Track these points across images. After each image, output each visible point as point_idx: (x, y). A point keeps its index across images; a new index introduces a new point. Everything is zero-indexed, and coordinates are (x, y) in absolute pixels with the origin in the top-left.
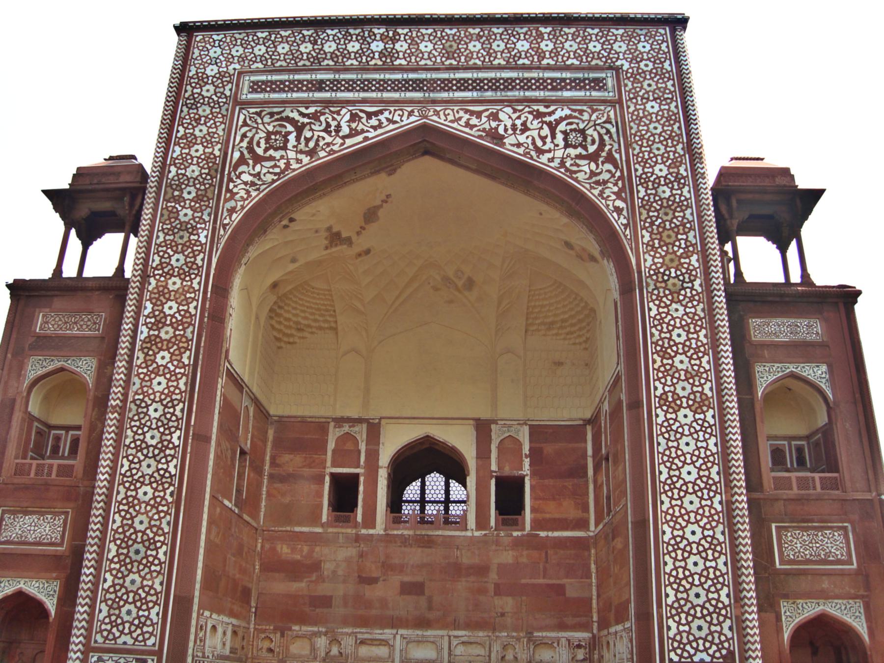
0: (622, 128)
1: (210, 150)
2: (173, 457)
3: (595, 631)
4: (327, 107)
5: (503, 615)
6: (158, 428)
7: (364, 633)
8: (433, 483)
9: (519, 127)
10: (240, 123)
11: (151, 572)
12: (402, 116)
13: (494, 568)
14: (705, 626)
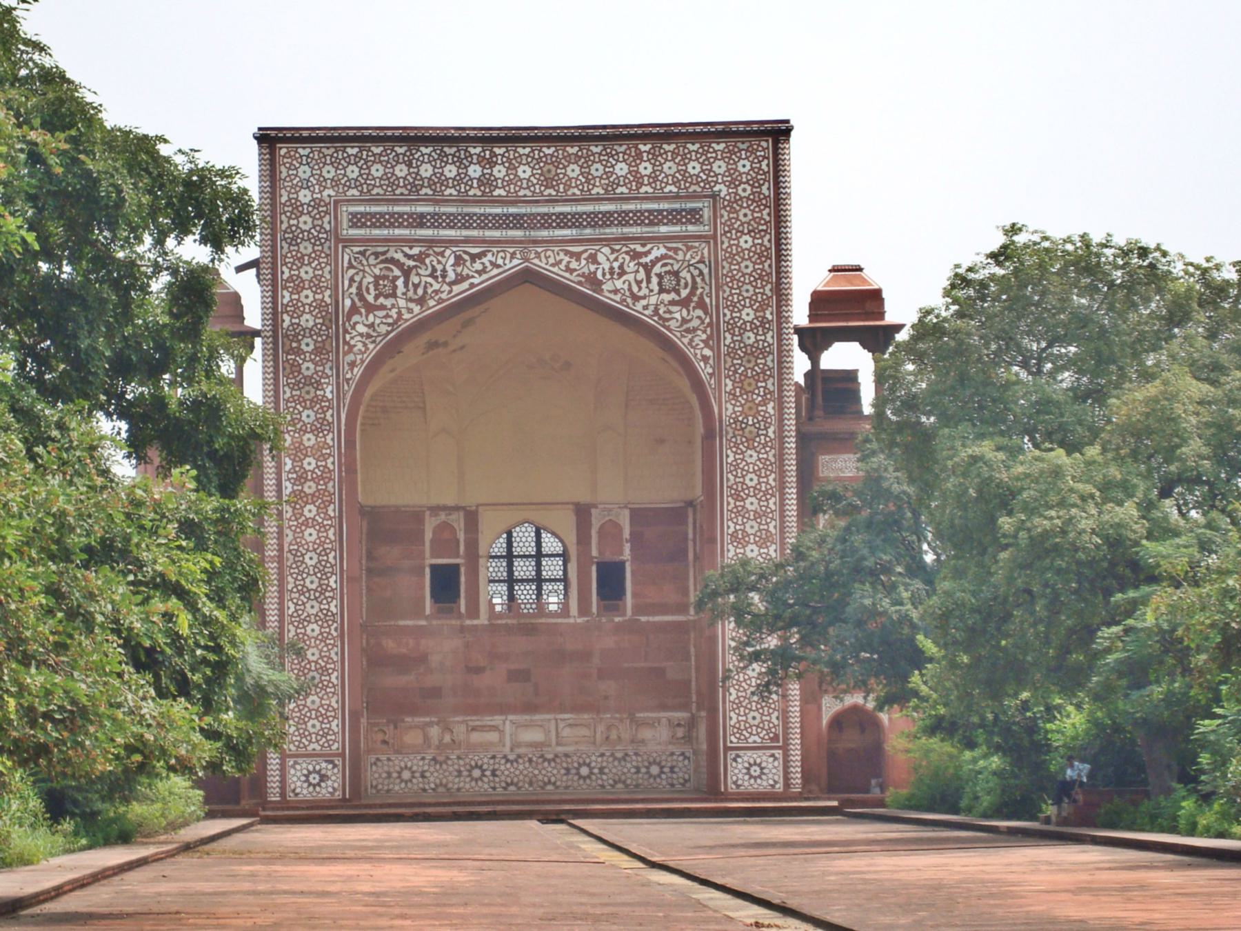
0: (715, 267)
1: (320, 297)
2: (333, 598)
4: (431, 247)
5: (606, 698)
6: (315, 574)
7: (475, 721)
9: (617, 270)
10: (346, 265)
11: (327, 693)
12: (504, 259)
14: (758, 716)
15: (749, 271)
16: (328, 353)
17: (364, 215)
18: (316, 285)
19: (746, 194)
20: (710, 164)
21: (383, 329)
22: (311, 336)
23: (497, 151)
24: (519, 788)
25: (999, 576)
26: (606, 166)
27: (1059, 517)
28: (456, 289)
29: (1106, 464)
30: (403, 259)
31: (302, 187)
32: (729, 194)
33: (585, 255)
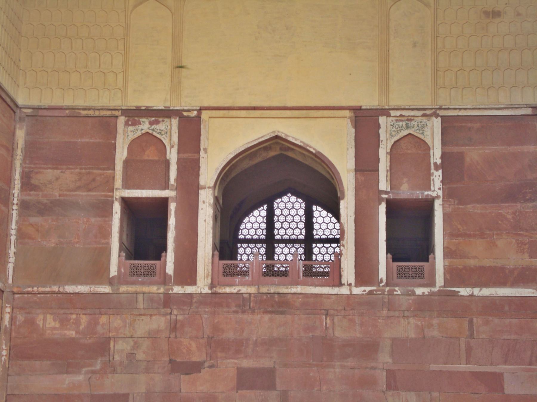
8: (286, 212)
13: (386, 346)
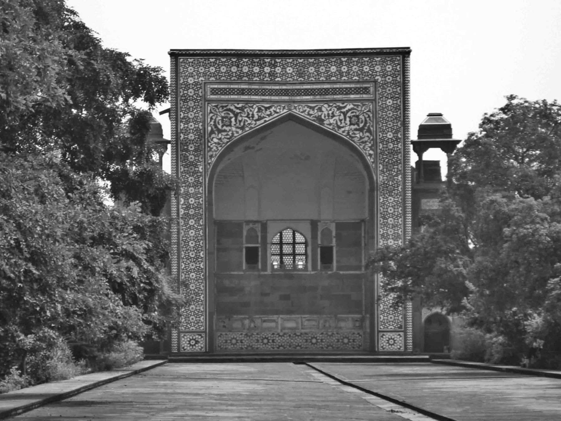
0: (375, 113)
2: (202, 261)
3: (364, 314)
4: (247, 104)
5: (324, 308)
9: (331, 115)
11: (199, 304)
15: (391, 115)
16: (200, 151)
17: (217, 89)
18: (195, 121)
19: (389, 81)
20: (374, 67)
21: (225, 140)
22: (193, 143)
23: (278, 61)
24: (285, 348)
25: (503, 255)
26: (326, 68)
27: (531, 228)
28: (258, 123)
29: (553, 204)
30: (235, 109)
31: (189, 76)
32: (382, 81)
33: (316, 108)
